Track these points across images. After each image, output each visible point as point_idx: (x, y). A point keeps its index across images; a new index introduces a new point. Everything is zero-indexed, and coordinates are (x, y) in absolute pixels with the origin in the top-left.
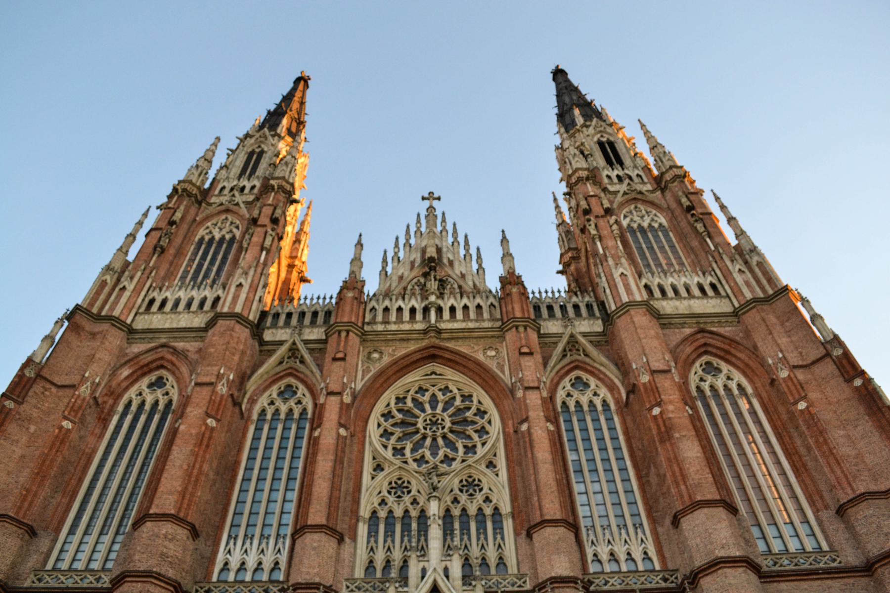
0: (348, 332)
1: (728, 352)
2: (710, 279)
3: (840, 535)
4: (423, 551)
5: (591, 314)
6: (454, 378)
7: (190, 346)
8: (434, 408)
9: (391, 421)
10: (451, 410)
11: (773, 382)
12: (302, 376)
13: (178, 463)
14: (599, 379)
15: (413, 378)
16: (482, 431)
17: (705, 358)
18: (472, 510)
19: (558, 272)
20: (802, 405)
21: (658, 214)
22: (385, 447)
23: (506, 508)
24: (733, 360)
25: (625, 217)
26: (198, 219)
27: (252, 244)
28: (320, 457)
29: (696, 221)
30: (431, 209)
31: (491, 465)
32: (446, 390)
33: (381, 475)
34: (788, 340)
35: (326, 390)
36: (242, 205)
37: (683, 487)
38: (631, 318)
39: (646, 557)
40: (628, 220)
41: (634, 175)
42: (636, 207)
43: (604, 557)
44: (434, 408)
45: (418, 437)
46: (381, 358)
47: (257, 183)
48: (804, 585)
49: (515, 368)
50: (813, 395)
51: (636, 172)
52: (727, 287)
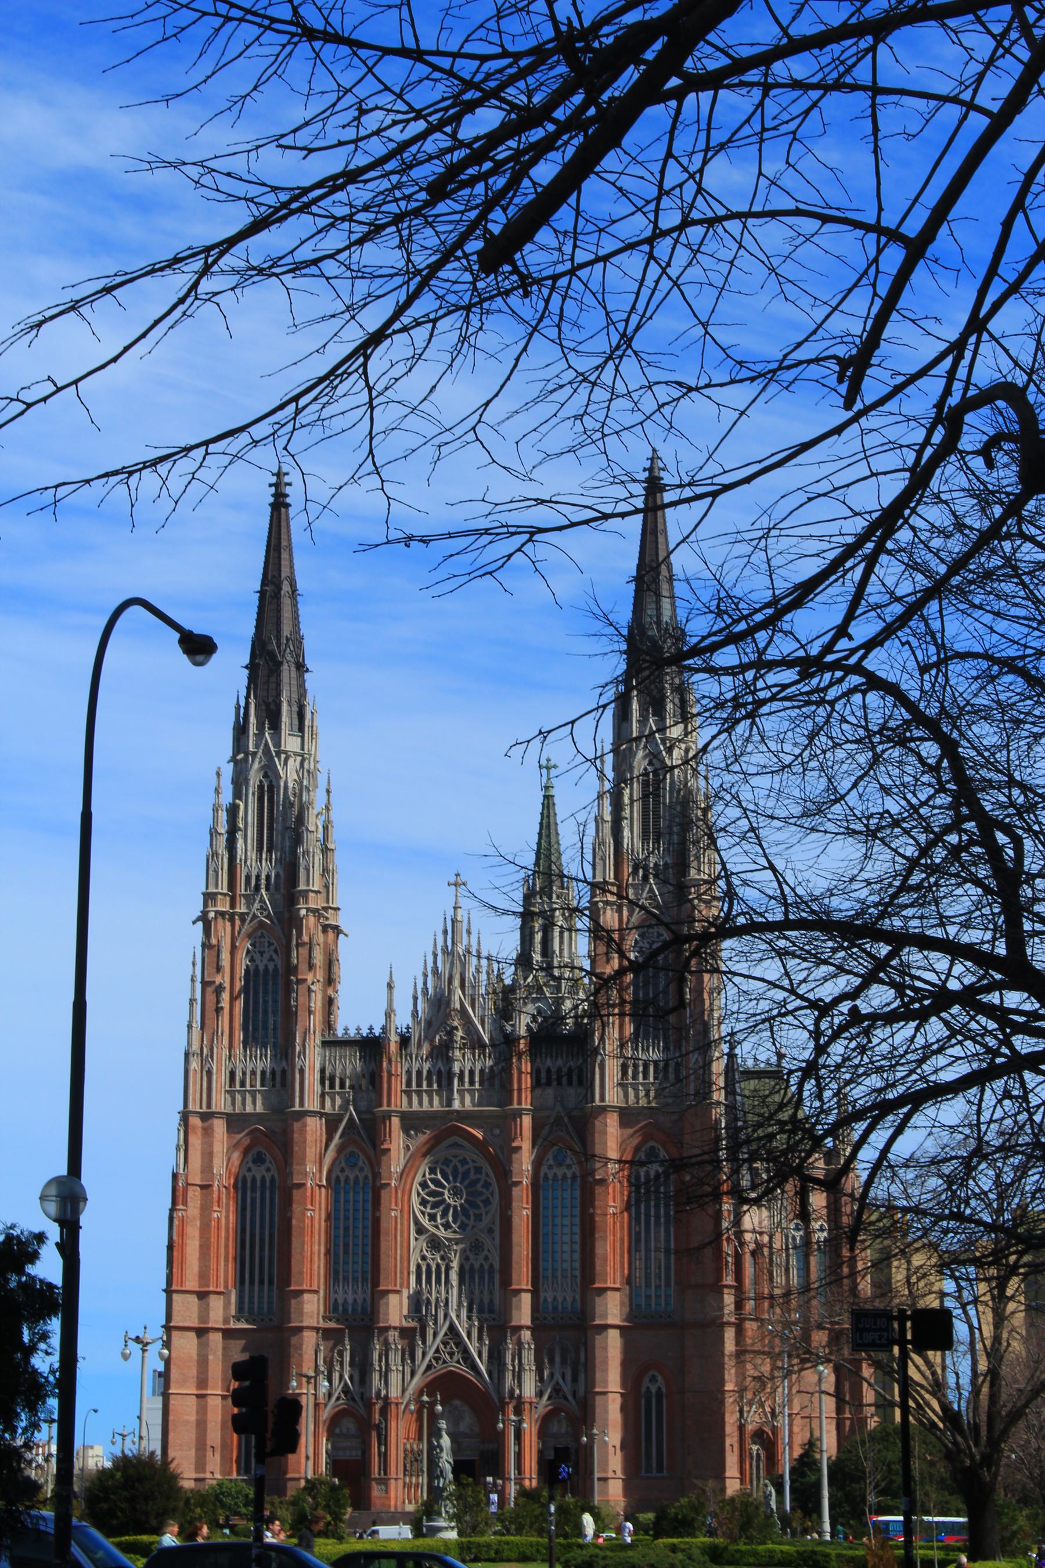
10: (467, 1182)
16: (487, 1202)
17: (652, 1143)
18: (477, 1266)
22: (423, 1213)
23: (497, 1266)
31: (491, 1231)
32: (464, 1162)
39: (574, 1299)
43: (550, 1300)
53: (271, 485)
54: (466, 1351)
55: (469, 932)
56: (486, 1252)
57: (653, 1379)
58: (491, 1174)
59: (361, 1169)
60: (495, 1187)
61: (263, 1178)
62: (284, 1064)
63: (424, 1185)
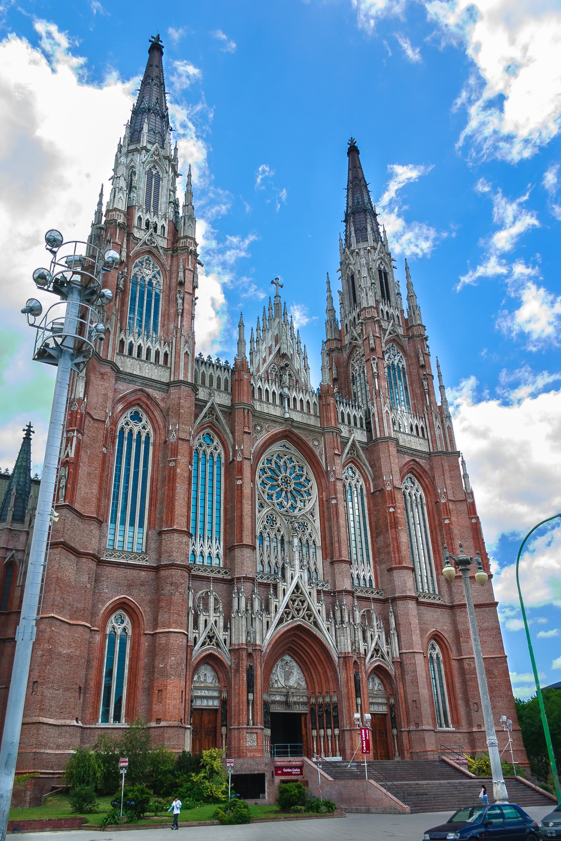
0: (248, 410)
1: (421, 476)
3: (445, 589)
4: (292, 566)
7: (157, 395)
8: (286, 471)
9: (265, 475)
11: (437, 502)
12: (217, 430)
13: (182, 496)
14: (361, 472)
15: (276, 448)
20: (447, 522)
21: (403, 357)
23: (319, 543)
24: (422, 481)
26: (131, 255)
27: (185, 311)
28: (244, 501)
29: (425, 379)
33: (265, 510)
34: (450, 482)
35: (242, 454)
36: (161, 251)
37: (397, 555)
38: (388, 447)
41: (395, 315)
42: (392, 346)
45: (279, 489)
46: (261, 431)
48: (429, 609)
49: (330, 461)
50: (454, 519)
51: (397, 313)
52: (429, 434)
54: (309, 609)
56: (309, 531)
57: (433, 648)
59: (215, 449)
60: (313, 483)
61: (139, 433)
62: (167, 349)
63: (263, 470)
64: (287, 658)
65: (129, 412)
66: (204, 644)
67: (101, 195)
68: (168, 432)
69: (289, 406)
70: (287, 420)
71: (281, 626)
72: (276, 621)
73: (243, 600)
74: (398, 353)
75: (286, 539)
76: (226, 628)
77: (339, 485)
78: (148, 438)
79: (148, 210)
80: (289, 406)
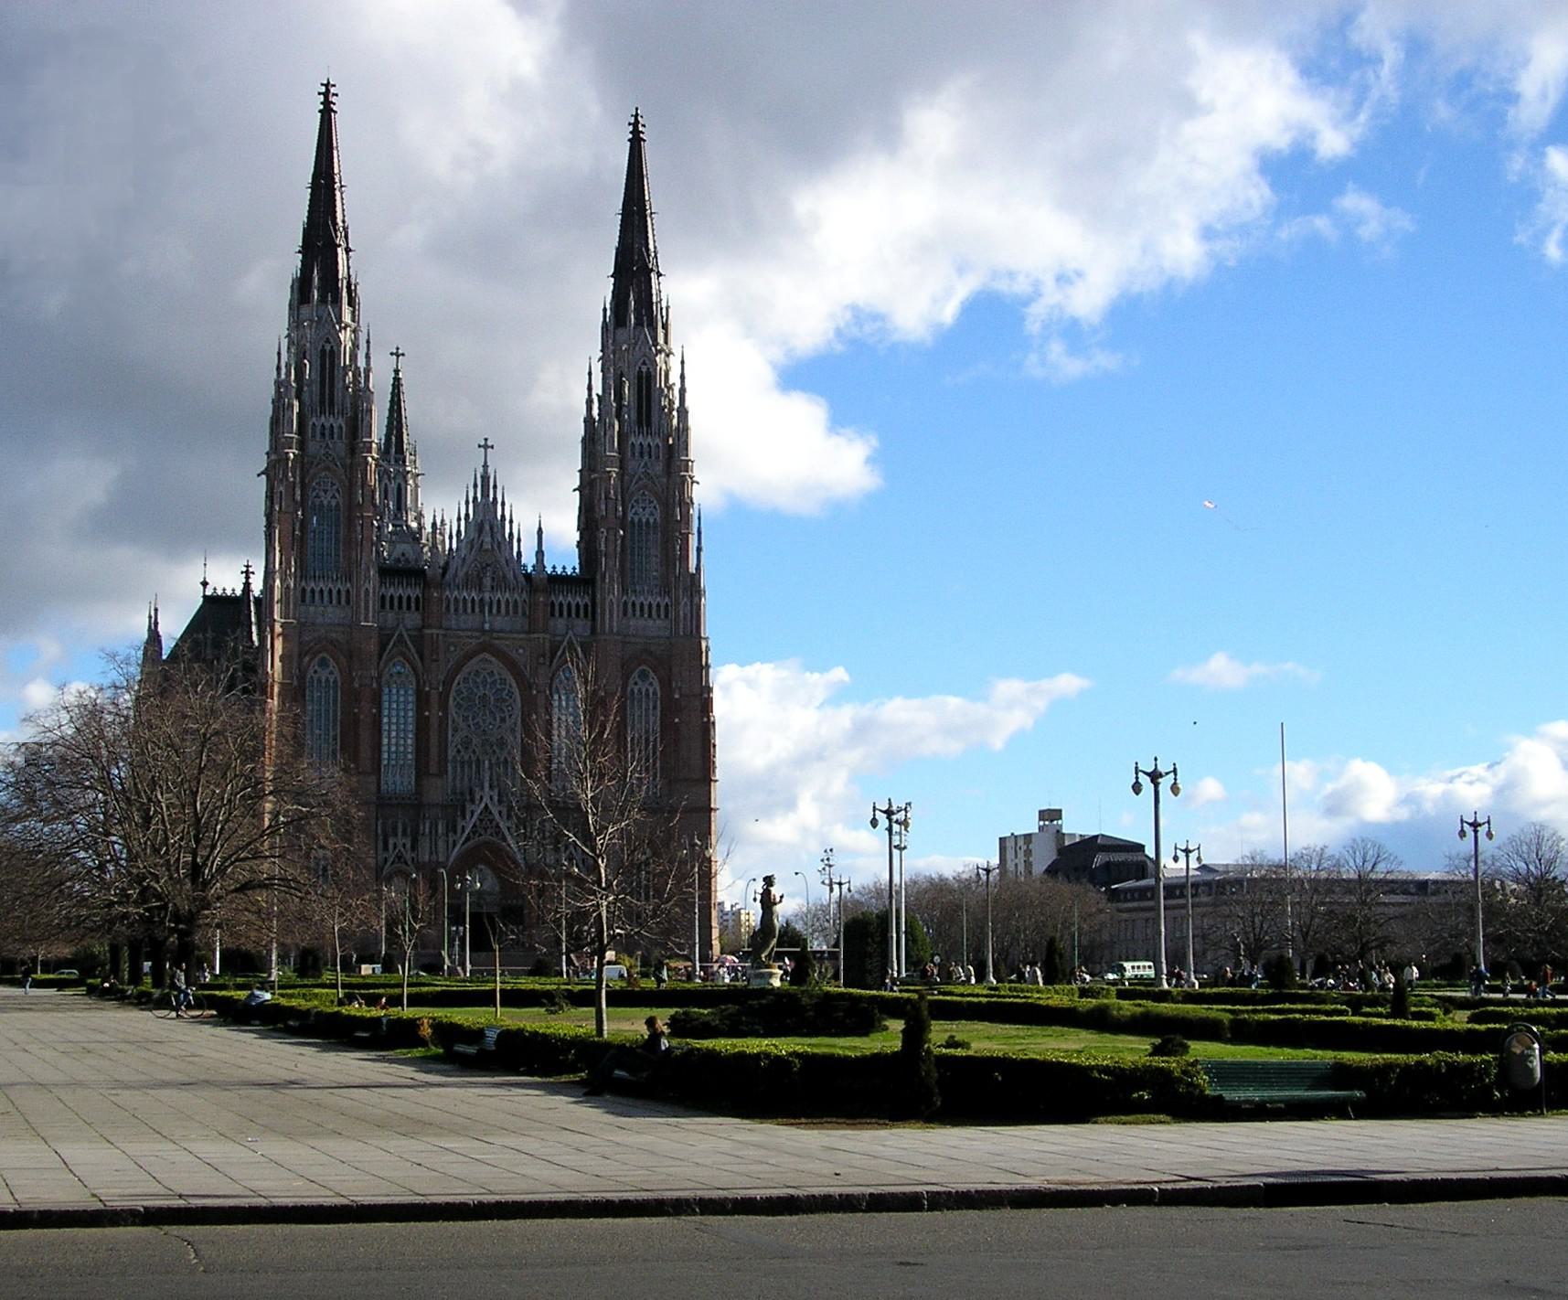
2: (667, 600)
4: (482, 788)
5: (586, 616)
6: (496, 666)
8: (485, 686)
19: (575, 490)
25: (633, 507)
30: (485, 466)
31: (513, 731)
35: (430, 684)
40: (633, 511)
44: (485, 686)
47: (341, 421)
51: (657, 441)
53: (319, 94)
54: (498, 826)
55: (495, 487)
58: (514, 685)
59: (407, 677)
62: (349, 585)
63: (459, 692)
64: (483, 867)
65: (317, 659)
66: (392, 863)
67: (279, 354)
68: (353, 679)
69: (490, 611)
70: (483, 631)
71: (469, 843)
72: (463, 839)
73: (427, 825)
74: (651, 502)
75: (481, 758)
76: (414, 848)
77: (541, 701)
78: (335, 681)
79: (322, 412)
80: (490, 611)
